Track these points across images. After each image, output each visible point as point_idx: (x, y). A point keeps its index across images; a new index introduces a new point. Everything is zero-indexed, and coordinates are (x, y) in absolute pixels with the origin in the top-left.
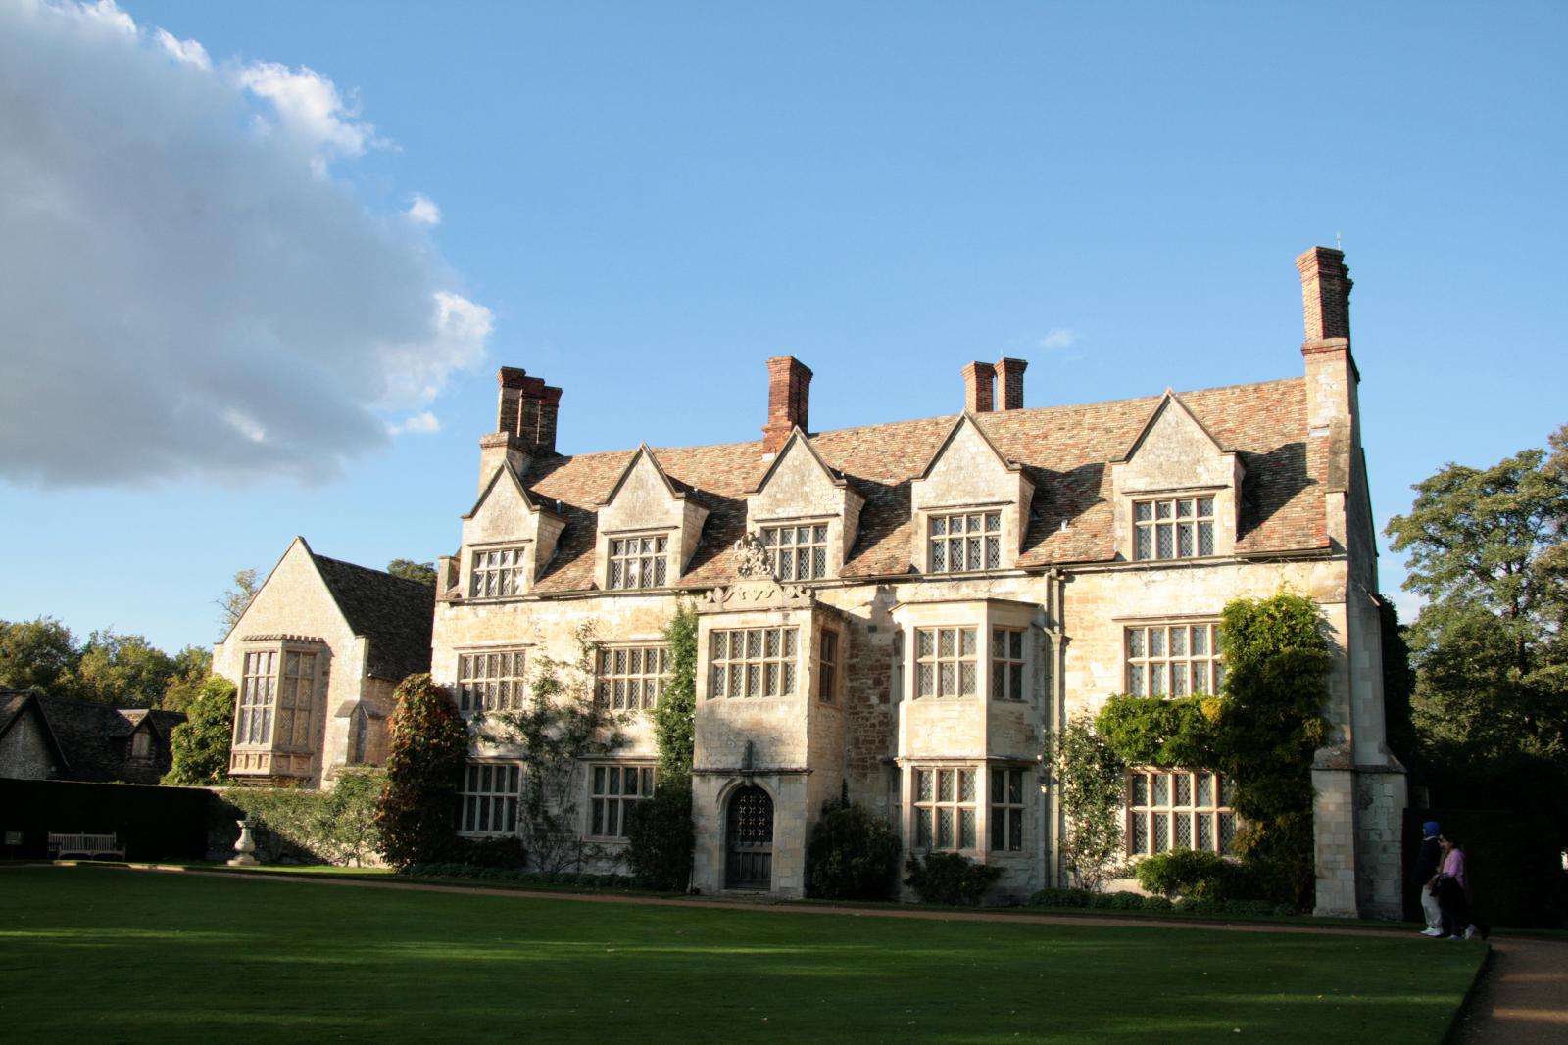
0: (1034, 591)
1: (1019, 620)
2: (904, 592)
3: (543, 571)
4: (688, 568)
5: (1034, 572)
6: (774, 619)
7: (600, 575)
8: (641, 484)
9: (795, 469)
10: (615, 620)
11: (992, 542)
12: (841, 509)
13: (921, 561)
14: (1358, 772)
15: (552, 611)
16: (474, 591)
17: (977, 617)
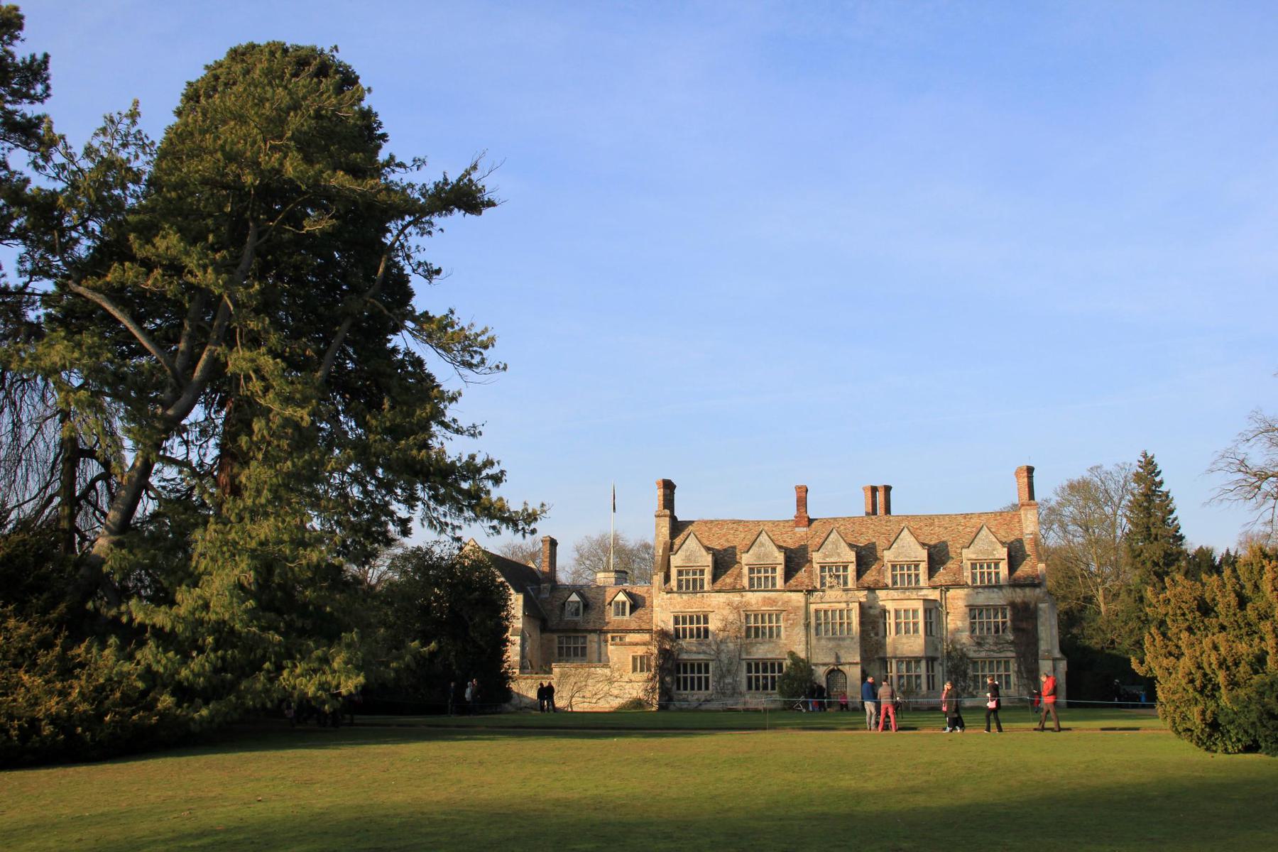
0: (934, 595)
1: (931, 606)
2: (881, 594)
3: (715, 578)
4: (786, 582)
5: (934, 588)
6: (843, 605)
7: (746, 582)
8: (762, 545)
9: (833, 543)
10: (753, 601)
11: (917, 576)
12: (854, 559)
13: (889, 581)
14: (1054, 660)
15: (721, 598)
16: (680, 587)
17: (919, 606)
